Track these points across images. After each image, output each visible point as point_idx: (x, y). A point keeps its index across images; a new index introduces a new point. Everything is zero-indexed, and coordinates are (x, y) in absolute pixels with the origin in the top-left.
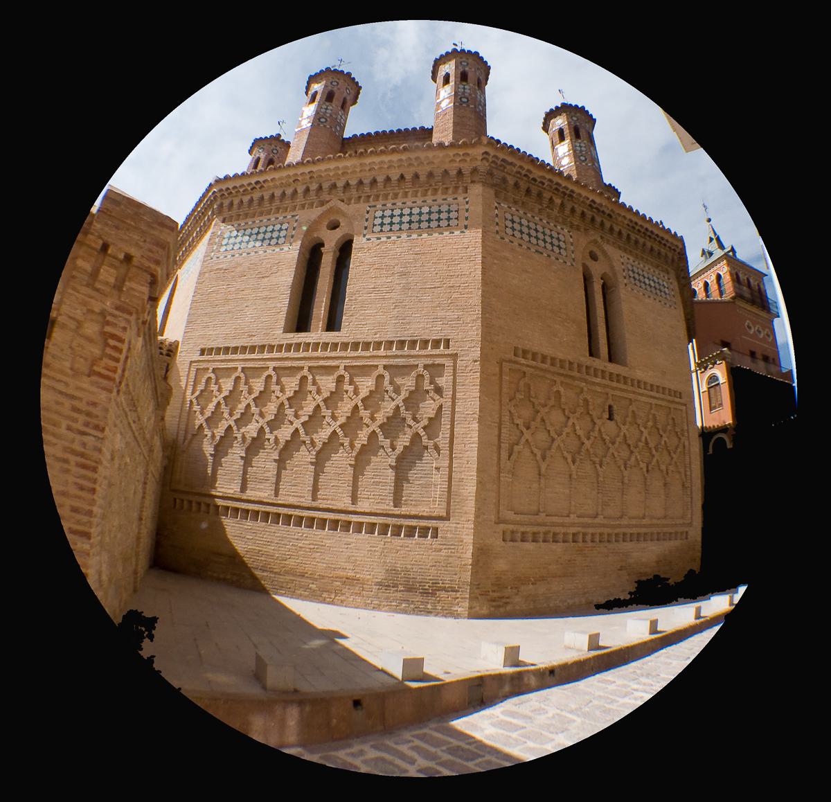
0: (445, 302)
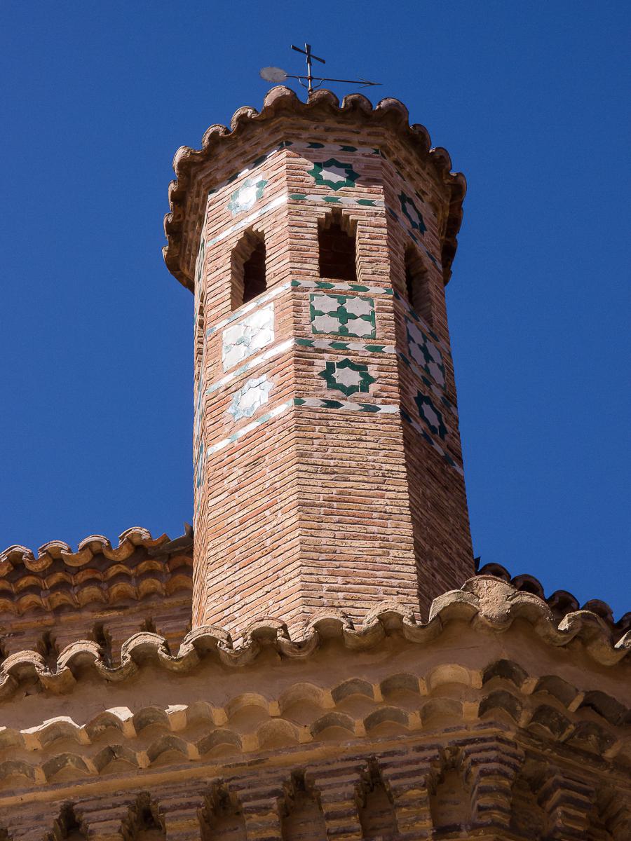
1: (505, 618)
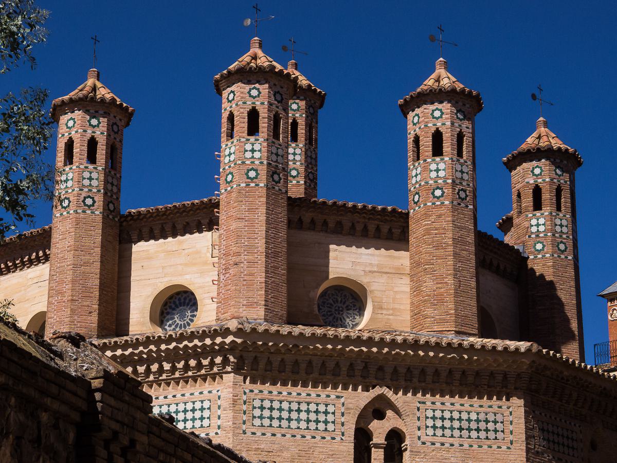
1: (537, 352)
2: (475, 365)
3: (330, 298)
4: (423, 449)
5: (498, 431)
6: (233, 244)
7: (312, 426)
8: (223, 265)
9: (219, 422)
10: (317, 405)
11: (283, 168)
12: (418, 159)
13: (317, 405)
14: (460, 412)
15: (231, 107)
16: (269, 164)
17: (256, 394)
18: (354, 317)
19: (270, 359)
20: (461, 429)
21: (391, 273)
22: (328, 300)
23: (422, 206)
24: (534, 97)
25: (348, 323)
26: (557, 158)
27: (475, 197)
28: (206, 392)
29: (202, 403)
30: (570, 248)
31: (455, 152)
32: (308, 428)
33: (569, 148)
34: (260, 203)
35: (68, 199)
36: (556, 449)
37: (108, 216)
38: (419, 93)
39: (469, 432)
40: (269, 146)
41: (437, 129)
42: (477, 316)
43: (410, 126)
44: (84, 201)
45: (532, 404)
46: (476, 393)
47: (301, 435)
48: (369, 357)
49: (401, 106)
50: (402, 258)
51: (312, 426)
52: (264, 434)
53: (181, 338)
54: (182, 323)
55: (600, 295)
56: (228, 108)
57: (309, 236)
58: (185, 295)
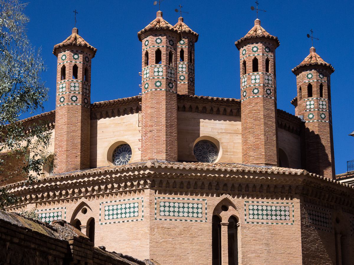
0: (287, 261)
1: (306, 175)
2: (274, 182)
3: (200, 147)
4: (248, 225)
5: (287, 216)
6: (149, 121)
7: (190, 215)
8: (144, 132)
9: (143, 214)
10: (193, 204)
11: (174, 80)
12: (245, 73)
13: (193, 204)
14: (267, 206)
15: (147, 49)
16: (167, 79)
17: (161, 199)
18: (213, 156)
19: (168, 181)
20: (267, 215)
21: (232, 133)
22: (199, 148)
23: (247, 98)
24: (308, 36)
25: (210, 160)
26: (320, 69)
27: (275, 92)
28: (136, 199)
29: (134, 204)
30: (327, 116)
31: (265, 69)
32: (188, 216)
33: (327, 63)
34: (162, 99)
35: (63, 97)
36: (317, 224)
37: (84, 106)
38: (245, 38)
39: (272, 217)
40: (167, 69)
41: (255, 57)
42: (277, 156)
43: (241, 56)
44: (71, 99)
45: (304, 201)
46: (275, 196)
47: (185, 220)
48: (219, 179)
49: (236, 45)
50: (237, 125)
51: (190, 215)
52: (166, 220)
53: (123, 171)
54: (124, 161)
55: (350, 135)
56: (145, 49)
57: (189, 115)
58: (125, 146)
